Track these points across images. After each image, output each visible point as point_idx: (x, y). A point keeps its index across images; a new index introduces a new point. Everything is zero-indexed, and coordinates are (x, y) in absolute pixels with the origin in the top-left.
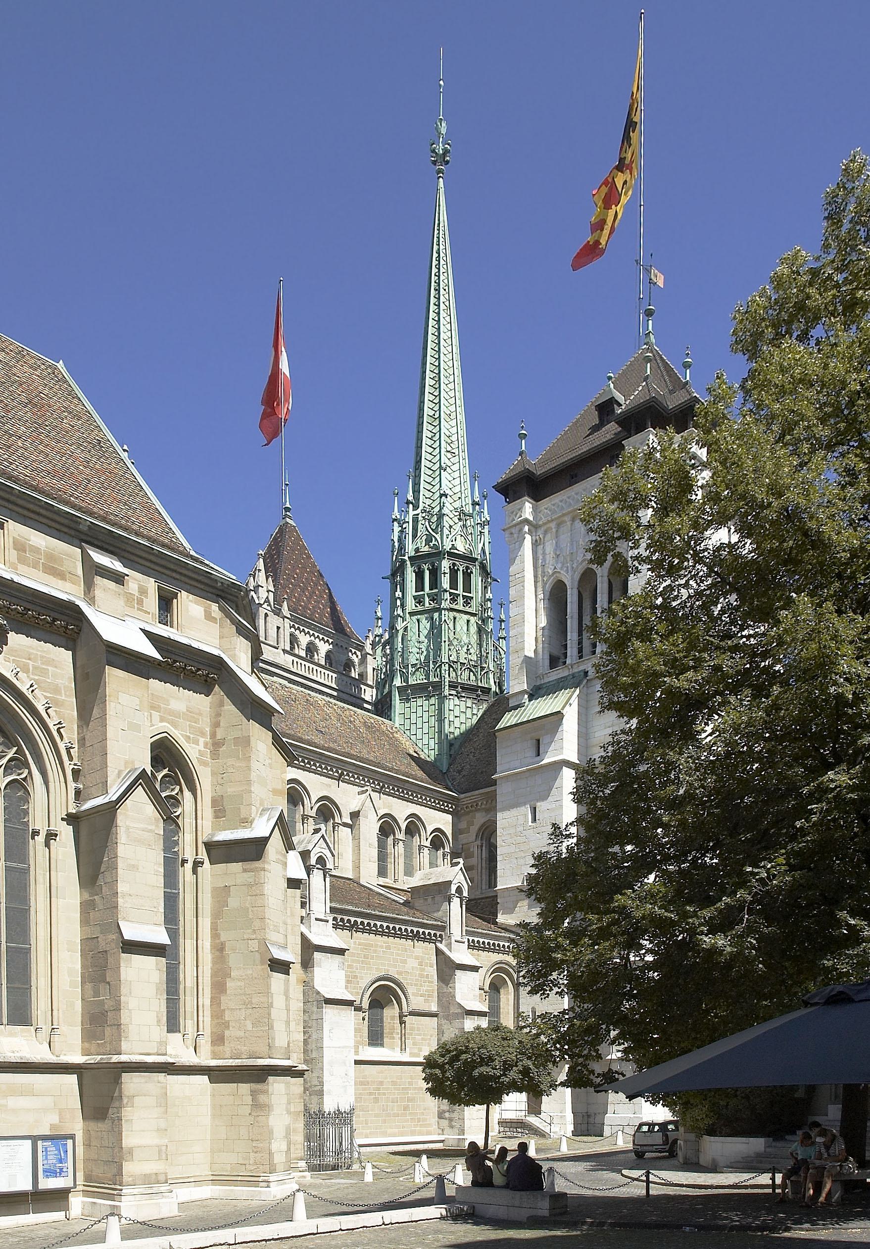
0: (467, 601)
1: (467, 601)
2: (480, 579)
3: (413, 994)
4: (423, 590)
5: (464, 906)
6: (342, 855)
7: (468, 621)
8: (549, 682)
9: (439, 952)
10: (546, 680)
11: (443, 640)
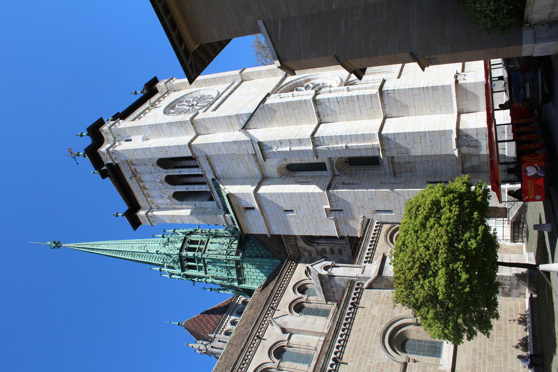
0: (202, 243)
1: (202, 243)
2: (192, 236)
4: (196, 266)
5: (339, 265)
6: (308, 343)
7: (211, 243)
8: (221, 201)
9: (370, 287)
10: (220, 203)
11: (215, 258)
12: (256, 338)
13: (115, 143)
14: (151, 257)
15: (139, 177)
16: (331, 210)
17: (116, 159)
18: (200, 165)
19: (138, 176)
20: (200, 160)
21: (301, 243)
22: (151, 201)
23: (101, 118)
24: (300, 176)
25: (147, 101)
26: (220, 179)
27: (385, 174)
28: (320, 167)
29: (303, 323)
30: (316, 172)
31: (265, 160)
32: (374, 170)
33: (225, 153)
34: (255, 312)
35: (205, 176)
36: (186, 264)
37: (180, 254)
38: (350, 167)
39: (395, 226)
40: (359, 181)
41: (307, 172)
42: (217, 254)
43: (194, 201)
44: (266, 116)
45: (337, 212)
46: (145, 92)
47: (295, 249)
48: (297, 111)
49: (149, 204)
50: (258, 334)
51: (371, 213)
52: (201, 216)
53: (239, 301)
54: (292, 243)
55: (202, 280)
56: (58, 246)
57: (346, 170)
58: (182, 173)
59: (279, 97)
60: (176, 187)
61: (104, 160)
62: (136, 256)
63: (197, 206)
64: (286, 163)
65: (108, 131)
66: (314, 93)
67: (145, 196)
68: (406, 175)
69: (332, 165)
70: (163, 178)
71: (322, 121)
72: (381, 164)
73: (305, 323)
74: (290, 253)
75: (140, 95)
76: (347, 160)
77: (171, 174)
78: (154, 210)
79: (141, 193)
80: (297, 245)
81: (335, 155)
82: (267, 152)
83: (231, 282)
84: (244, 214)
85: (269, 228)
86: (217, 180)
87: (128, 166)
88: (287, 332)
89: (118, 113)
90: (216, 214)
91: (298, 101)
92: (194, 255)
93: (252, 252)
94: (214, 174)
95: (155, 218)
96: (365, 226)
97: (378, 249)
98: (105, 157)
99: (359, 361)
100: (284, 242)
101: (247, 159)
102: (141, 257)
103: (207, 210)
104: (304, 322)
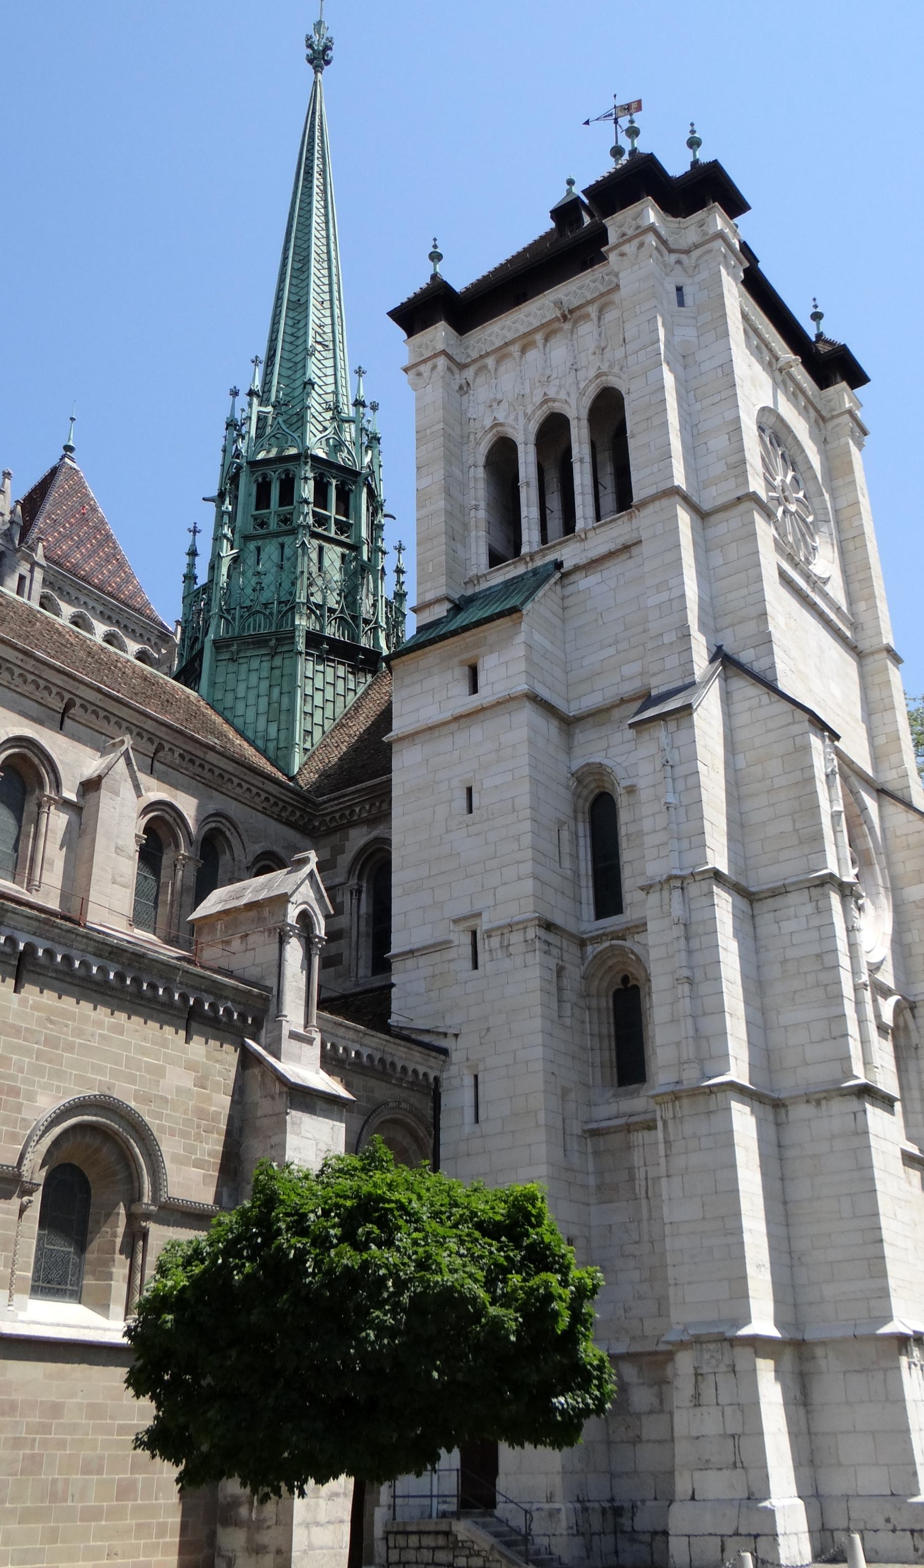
3: (176, 1159)
5: (316, 961)
7: (343, 556)
8: (490, 588)
9: (247, 1059)
10: (484, 585)
11: (299, 570)
12: (67, 696)
13: (671, 251)
14: (291, 364)
16: (474, 934)
17: (622, 255)
18: (606, 523)
19: (567, 326)
20: (620, 522)
21: (358, 838)
22: (485, 367)
25: (796, 354)
26: (563, 587)
27: (589, 1104)
29: (117, 848)
30: (591, 884)
31: (631, 726)
32: (602, 1067)
34: (136, 694)
35: (567, 540)
36: (274, 476)
37: (306, 458)
38: (611, 994)
39: (430, 1135)
40: (568, 1021)
41: (589, 858)
42: (310, 574)
43: (488, 505)
44: (768, 731)
45: (469, 949)
46: (823, 348)
47: (341, 817)
48: (787, 825)
50: (78, 702)
51: (468, 1059)
52: (442, 527)
53: (149, 639)
54: (357, 810)
55: (226, 527)
56: (315, 58)
57: (601, 979)
58: (576, 468)
59: (829, 770)
60: (532, 449)
61: (620, 216)
62: (291, 314)
63: (473, 513)
64: (620, 790)
65: (711, 231)
66: (845, 879)
67: (500, 348)
68: (591, 1168)
69: (615, 936)
70: (558, 407)
71: (756, 905)
72: (624, 1088)
73: (116, 852)
74: (325, 802)
75: (810, 330)
76: (632, 982)
77: (574, 432)
78: (457, 376)
79: (510, 336)
80: (353, 824)
81: (654, 946)
82: (661, 733)
83: (221, 617)
84: (456, 660)
85: (411, 737)
87: (598, 294)
88: (87, 797)
89: (758, 261)
90: (450, 573)
91: (821, 829)
92: (306, 502)
93: (319, 684)
94: (577, 569)
96: (426, 1039)
97: (358, 1081)
98: (629, 220)
99: (27, 1029)
100: (359, 786)
101: (629, 669)
102: (289, 331)
103: (459, 546)
104: (119, 850)
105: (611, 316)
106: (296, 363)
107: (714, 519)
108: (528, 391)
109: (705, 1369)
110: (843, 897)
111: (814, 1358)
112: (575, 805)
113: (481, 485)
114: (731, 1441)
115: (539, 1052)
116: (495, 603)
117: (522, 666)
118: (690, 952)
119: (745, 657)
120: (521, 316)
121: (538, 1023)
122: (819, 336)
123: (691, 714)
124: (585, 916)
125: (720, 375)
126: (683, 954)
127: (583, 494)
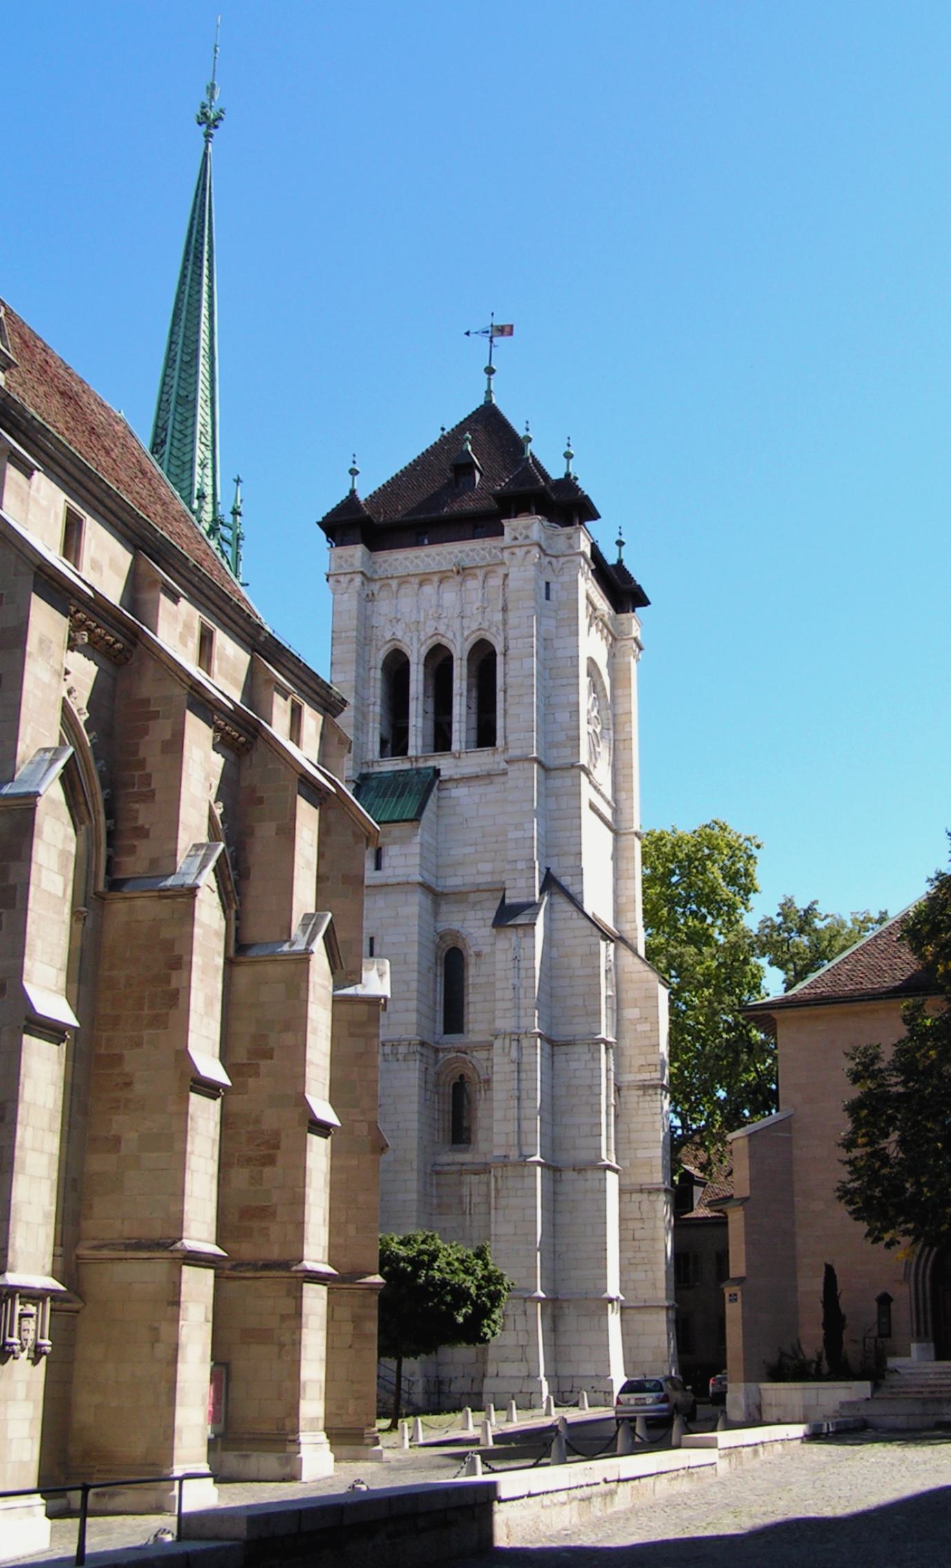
8: (381, 773)
10: (377, 769)
13: (546, 555)
14: (179, 463)
15: (451, 577)
19: (458, 579)
20: (486, 753)
22: (389, 585)
23: (599, 517)
24: (436, 975)
28: (454, 1017)
33: (511, 835)
43: (382, 701)
49: (381, 579)
60: (421, 668)
62: (180, 409)
64: (471, 951)
70: (444, 642)
72: (455, 1146)
79: (412, 570)
86: (437, 782)
94: (451, 780)
95: (347, 588)
102: (178, 427)
105: (495, 581)
106: (184, 463)
107: (553, 773)
108: (422, 620)
109: (509, 1312)
110: (607, 1049)
111: (561, 1308)
112: (436, 953)
113: (379, 685)
114: (520, 1349)
115: (415, 1125)
116: (393, 795)
117: (417, 860)
118: (519, 1080)
119: (565, 881)
120: (423, 554)
121: (415, 1107)
122: (620, 561)
123: (534, 929)
124: (438, 1032)
125: (569, 664)
126: (516, 1082)
127: (460, 722)
